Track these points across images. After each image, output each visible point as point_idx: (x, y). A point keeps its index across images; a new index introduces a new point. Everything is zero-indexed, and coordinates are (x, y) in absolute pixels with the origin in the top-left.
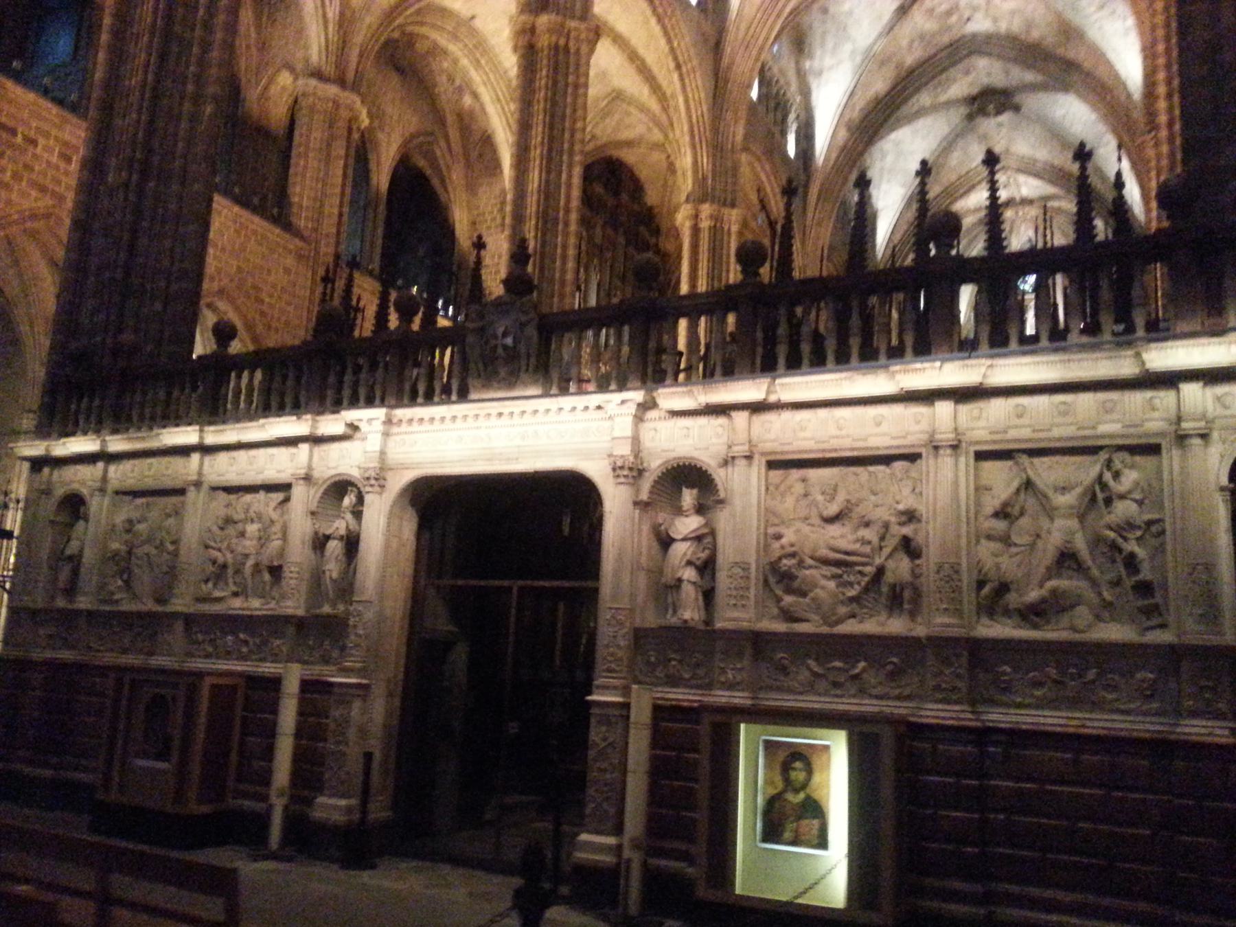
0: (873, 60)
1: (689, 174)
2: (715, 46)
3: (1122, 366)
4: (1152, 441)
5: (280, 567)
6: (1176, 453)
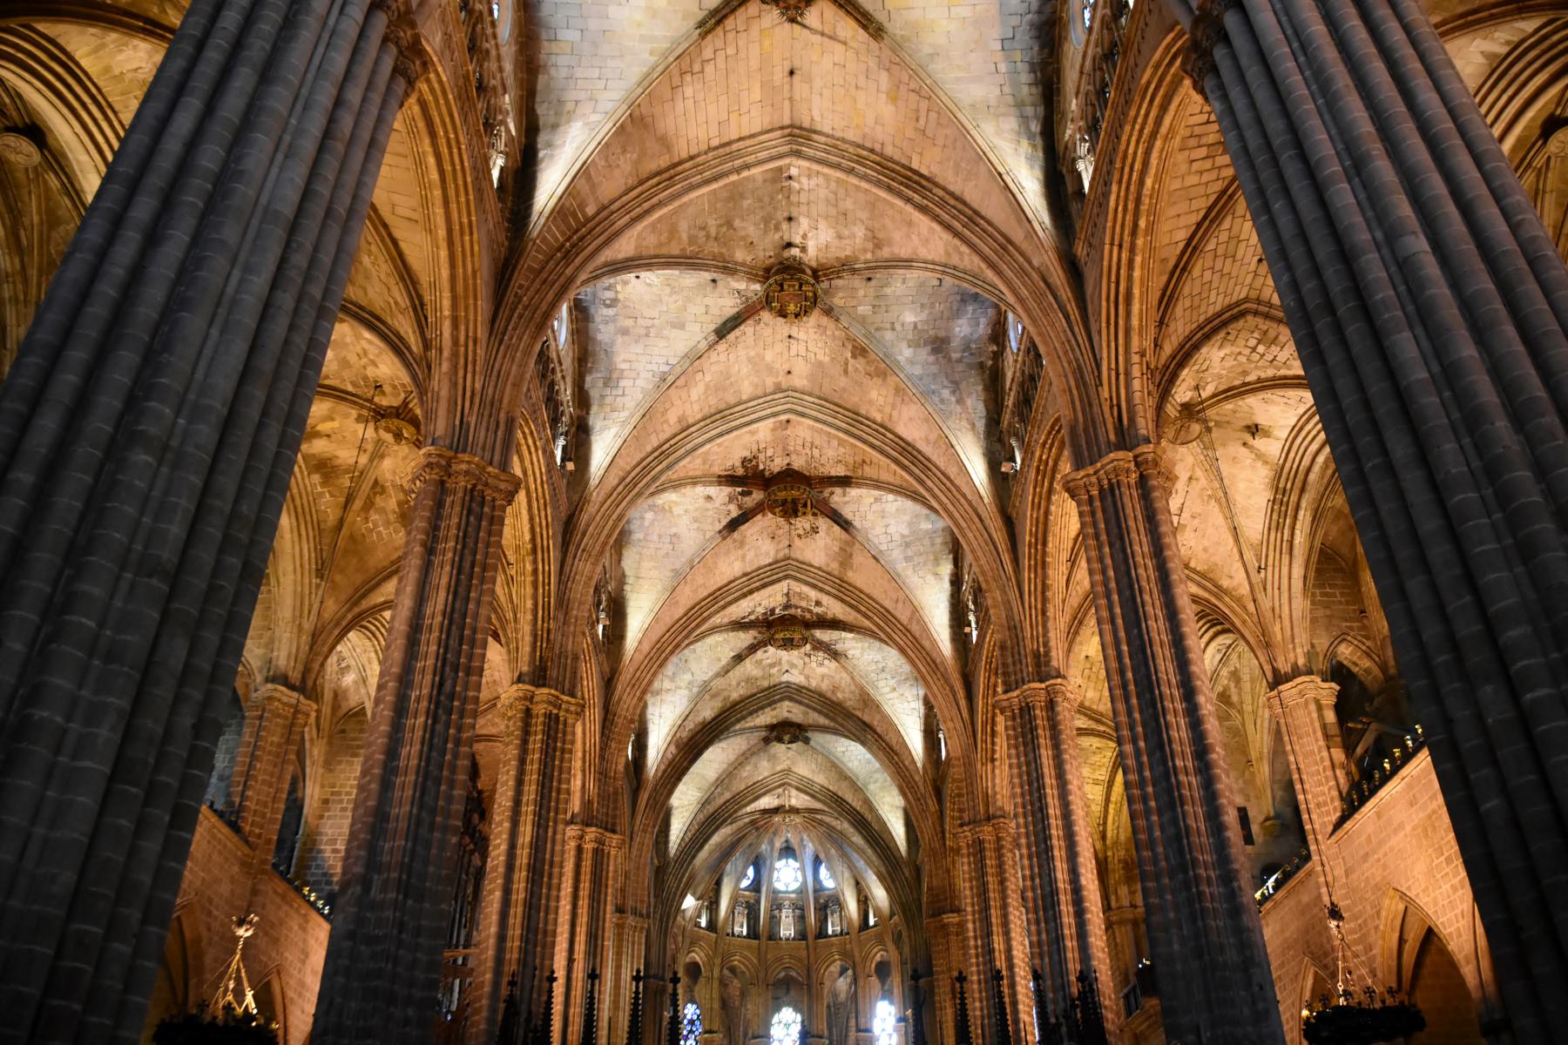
1: (578, 795)
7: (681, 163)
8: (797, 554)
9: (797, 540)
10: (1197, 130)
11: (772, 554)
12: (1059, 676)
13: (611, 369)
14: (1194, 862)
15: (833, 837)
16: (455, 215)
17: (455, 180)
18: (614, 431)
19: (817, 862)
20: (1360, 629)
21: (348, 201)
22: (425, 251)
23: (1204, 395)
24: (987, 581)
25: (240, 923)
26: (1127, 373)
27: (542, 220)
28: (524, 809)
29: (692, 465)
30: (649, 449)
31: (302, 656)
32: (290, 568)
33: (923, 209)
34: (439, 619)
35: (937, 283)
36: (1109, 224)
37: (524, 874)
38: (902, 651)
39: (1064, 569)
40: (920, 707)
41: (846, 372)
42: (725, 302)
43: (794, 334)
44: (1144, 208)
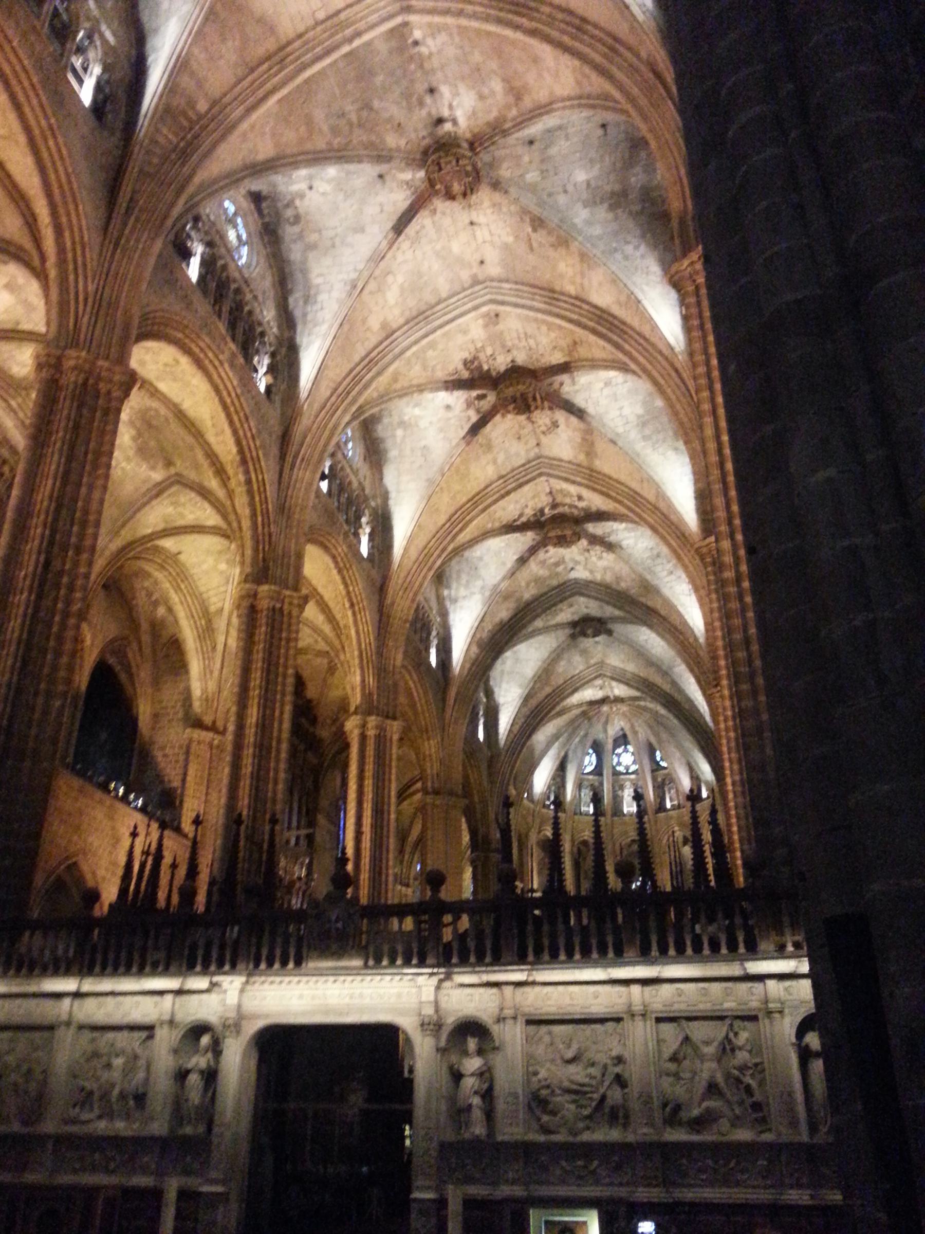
0: (498, 596)
1: (358, 690)
2: (381, 588)
3: (734, 969)
4: (753, 1013)
5: (144, 1095)
6: (767, 1021)
7: (289, 43)
8: (546, 452)
9: (542, 436)
11: (523, 453)
13: (308, 286)
17: (20, 82)
30: (357, 358)
33: (533, 33)
35: (600, 132)
41: (532, 249)
43: (475, 220)
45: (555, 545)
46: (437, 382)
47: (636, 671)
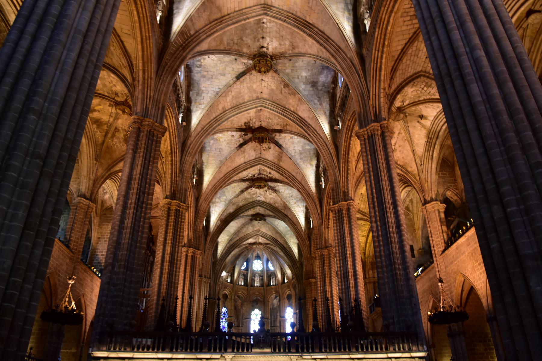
0: (230, 202)
7: (225, 16)
10: (407, 10)
11: (254, 156)
12: (352, 199)
13: (199, 89)
14: (395, 263)
15: (273, 253)
16: (144, 33)
18: (200, 111)
19: (268, 261)
20: (454, 186)
21: (105, 26)
22: (133, 45)
23: (405, 104)
24: (328, 167)
25: (70, 279)
26: (379, 96)
27: (175, 36)
28: (168, 241)
29: (227, 124)
30: (212, 118)
31: (90, 188)
32: (86, 158)
33: (310, 36)
34: (138, 176)
35: (314, 62)
36: (375, 43)
37: (168, 263)
38: (299, 190)
39: (355, 163)
40: (303, 209)
41: (281, 93)
42: (240, 67)
43: (264, 79)
44: (387, 37)
45: (256, 188)
46: (234, 128)
47: (271, 235)
